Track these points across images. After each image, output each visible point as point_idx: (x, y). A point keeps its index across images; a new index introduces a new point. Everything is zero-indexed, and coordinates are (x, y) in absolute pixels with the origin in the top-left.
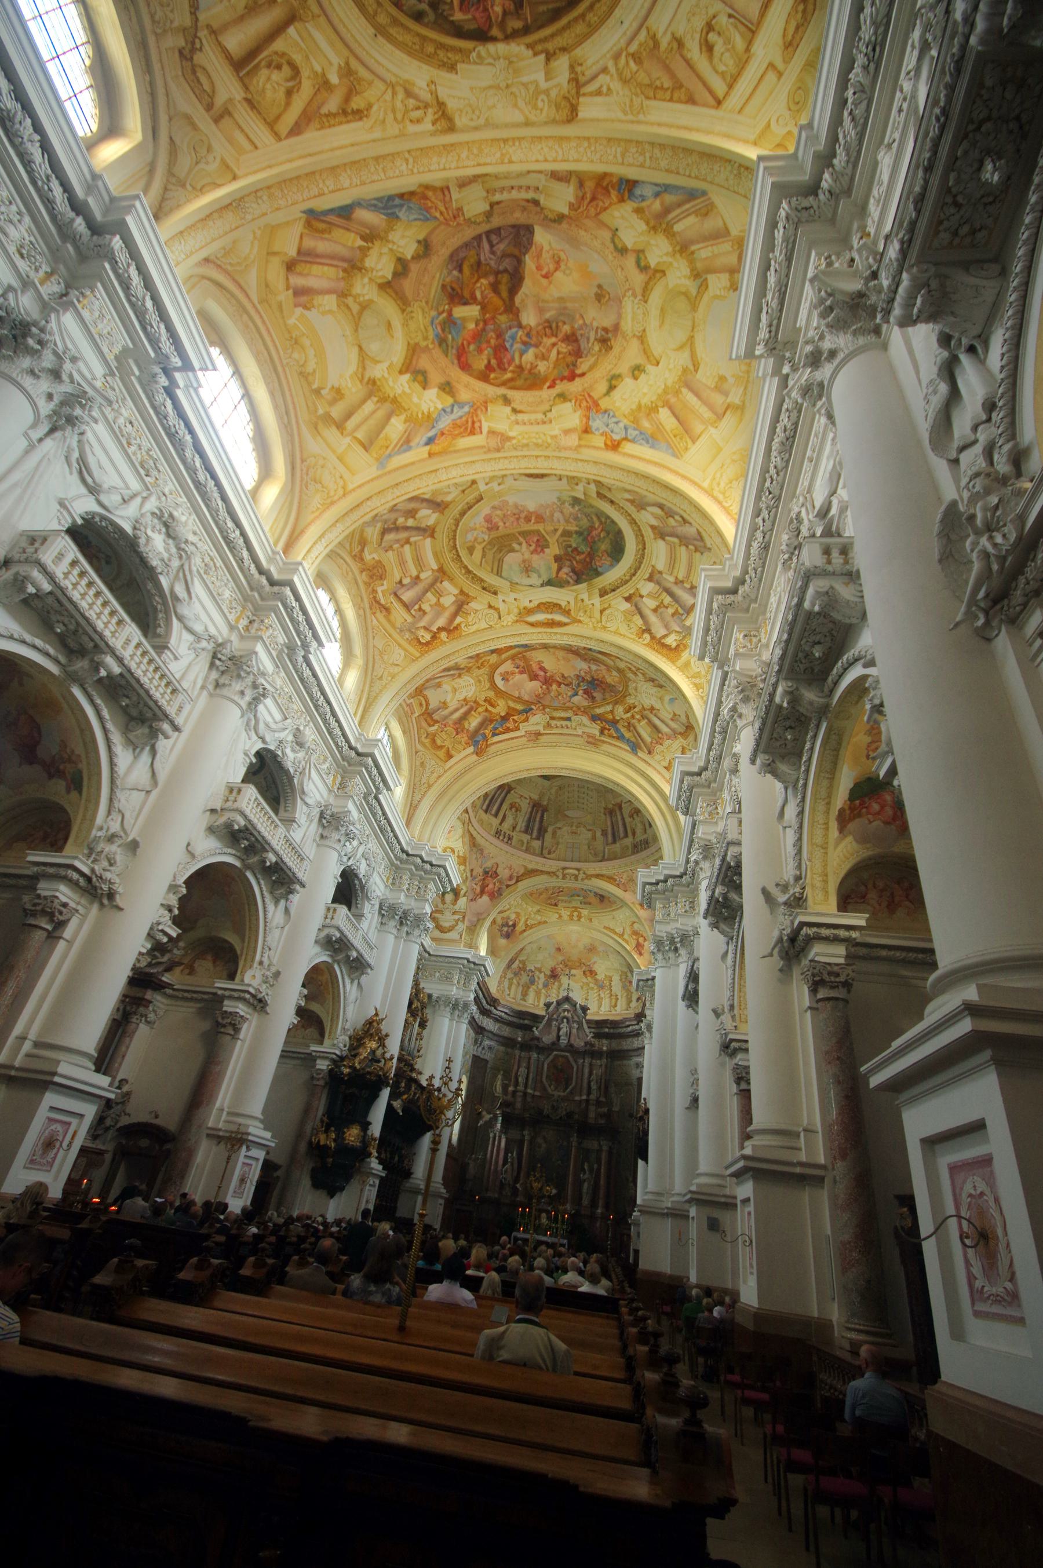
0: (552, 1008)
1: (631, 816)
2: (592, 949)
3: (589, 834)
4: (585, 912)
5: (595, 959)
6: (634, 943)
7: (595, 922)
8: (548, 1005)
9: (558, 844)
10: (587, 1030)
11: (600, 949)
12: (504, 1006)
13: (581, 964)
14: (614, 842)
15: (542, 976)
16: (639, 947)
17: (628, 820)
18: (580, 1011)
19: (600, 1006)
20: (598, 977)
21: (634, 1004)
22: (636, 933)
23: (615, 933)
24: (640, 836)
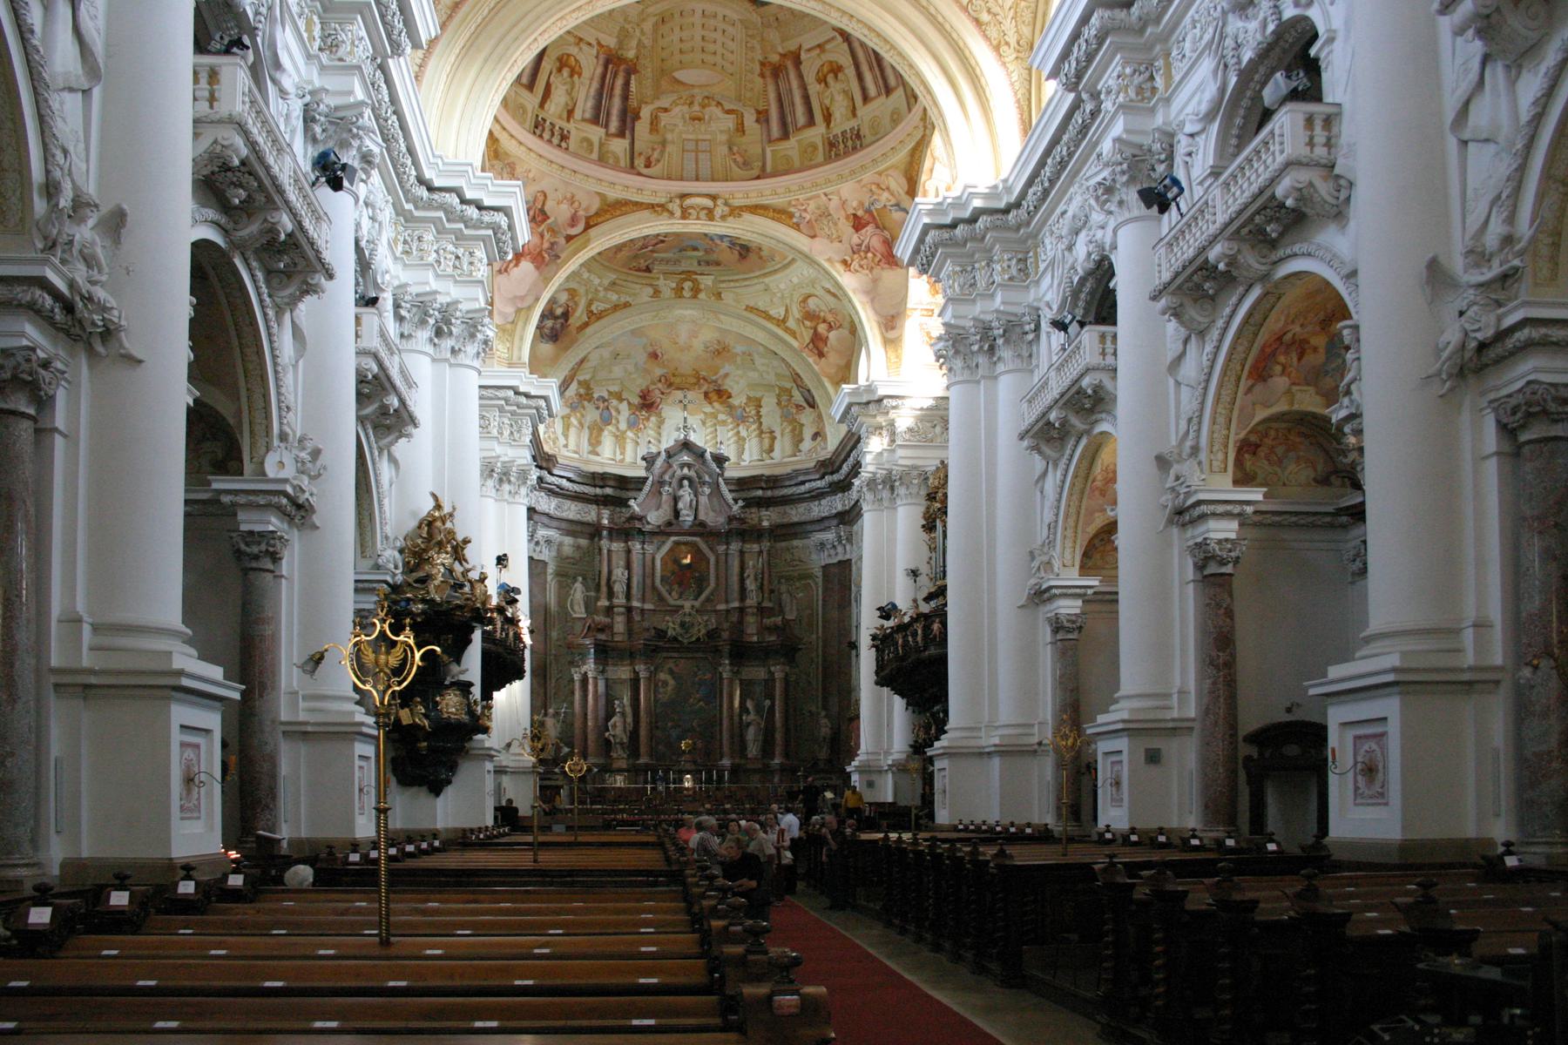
0: (659, 462)
1: (822, 80)
2: (720, 351)
3: (729, 122)
4: (706, 281)
5: (727, 368)
6: (807, 336)
7: (728, 297)
8: (650, 460)
9: (664, 143)
10: (729, 497)
11: (739, 349)
12: (566, 467)
13: (698, 379)
14: (785, 135)
15: (624, 406)
16: (817, 344)
17: (814, 88)
18: (714, 466)
19: (741, 452)
20: (735, 401)
21: (807, 444)
22: (810, 316)
23: (769, 317)
24: (842, 123)
